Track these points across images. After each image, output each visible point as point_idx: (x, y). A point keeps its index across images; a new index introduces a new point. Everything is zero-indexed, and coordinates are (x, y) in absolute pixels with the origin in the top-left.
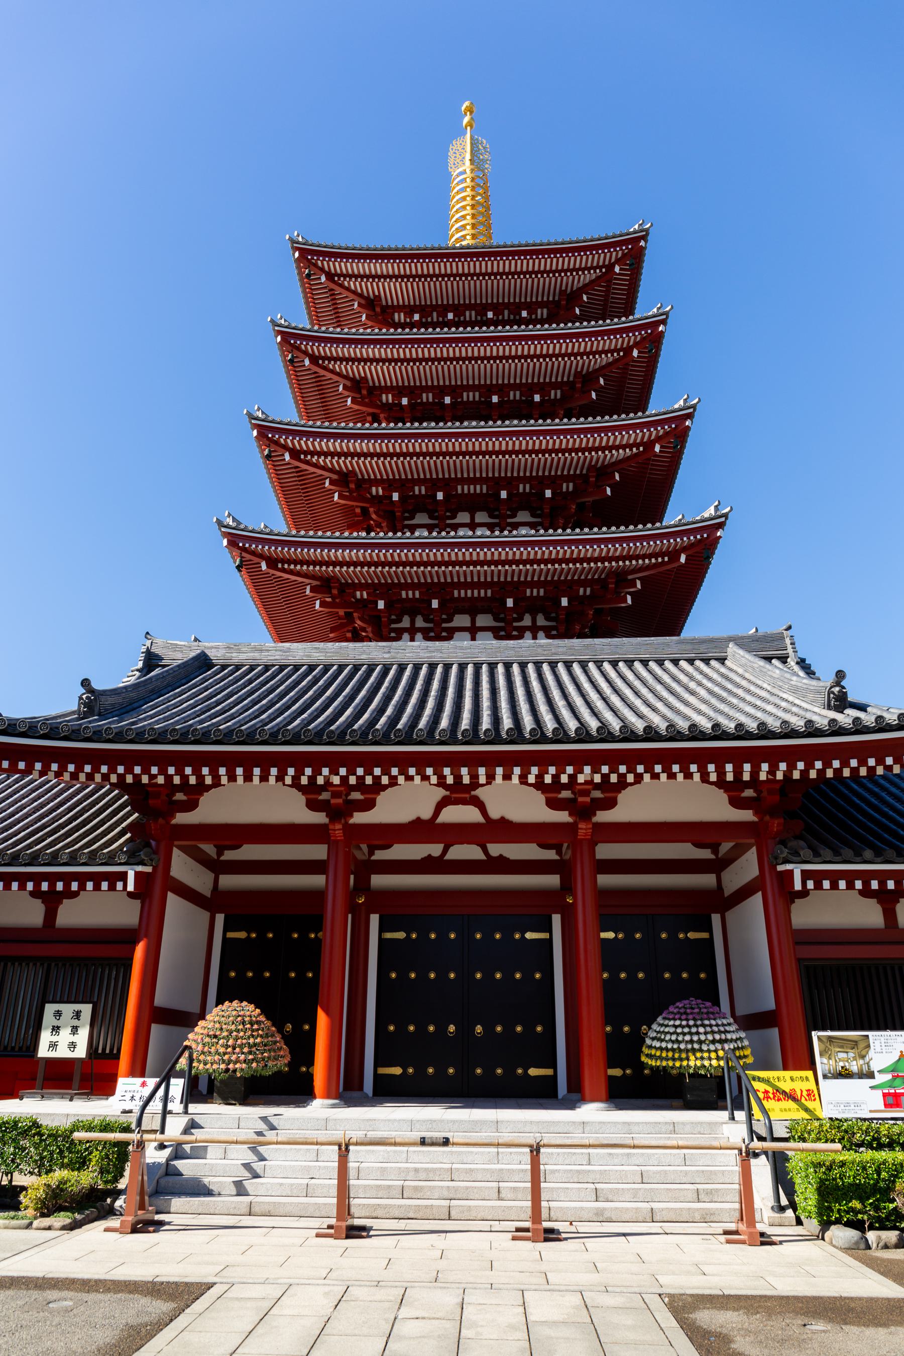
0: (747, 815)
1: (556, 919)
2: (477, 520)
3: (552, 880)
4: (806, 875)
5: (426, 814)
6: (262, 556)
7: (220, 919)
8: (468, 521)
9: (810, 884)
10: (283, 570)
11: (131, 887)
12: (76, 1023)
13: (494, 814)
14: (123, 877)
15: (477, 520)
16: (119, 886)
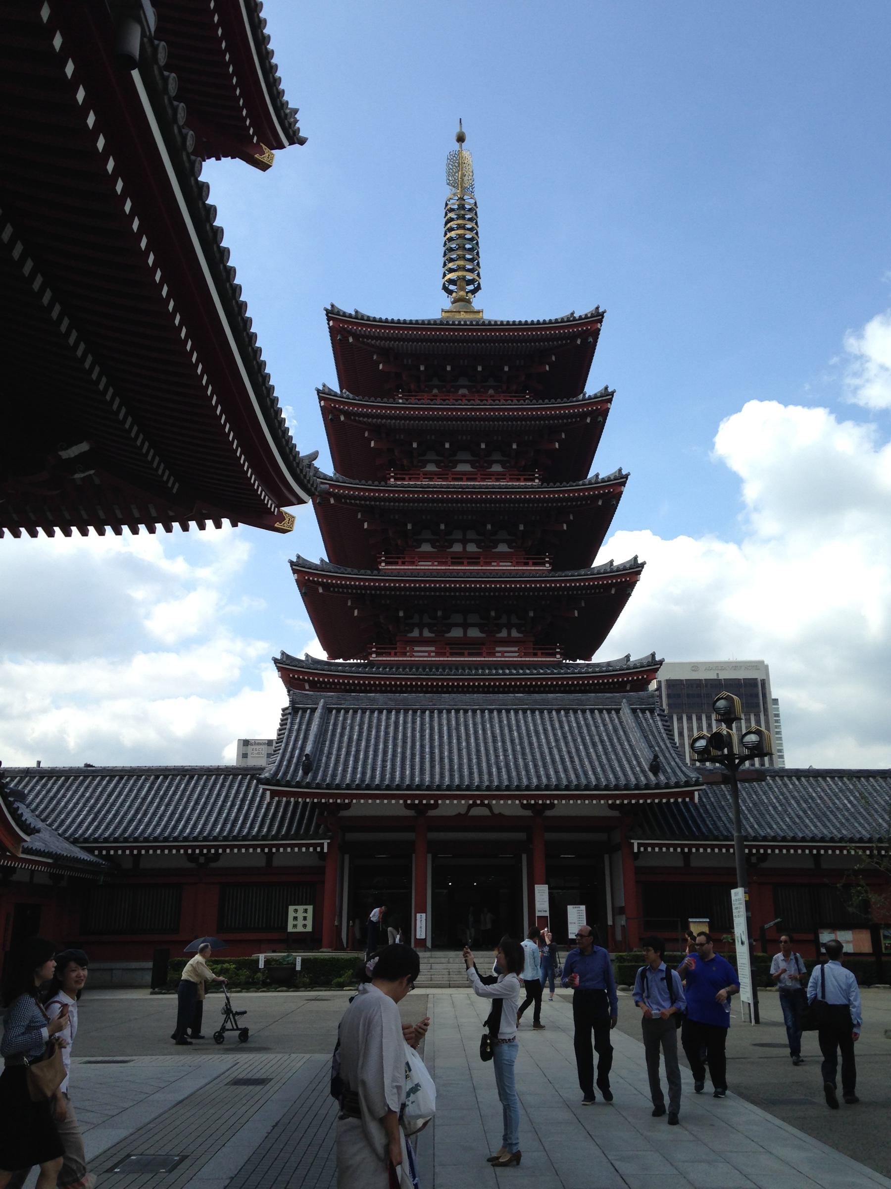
0: (616, 813)
1: (524, 857)
2: (468, 537)
3: (522, 836)
4: (639, 845)
5: (463, 811)
6: (319, 583)
7: (347, 857)
8: (461, 537)
9: (642, 849)
10: (334, 592)
11: (326, 850)
12: (305, 915)
13: (496, 811)
14: (322, 845)
15: (468, 537)
16: (319, 849)
